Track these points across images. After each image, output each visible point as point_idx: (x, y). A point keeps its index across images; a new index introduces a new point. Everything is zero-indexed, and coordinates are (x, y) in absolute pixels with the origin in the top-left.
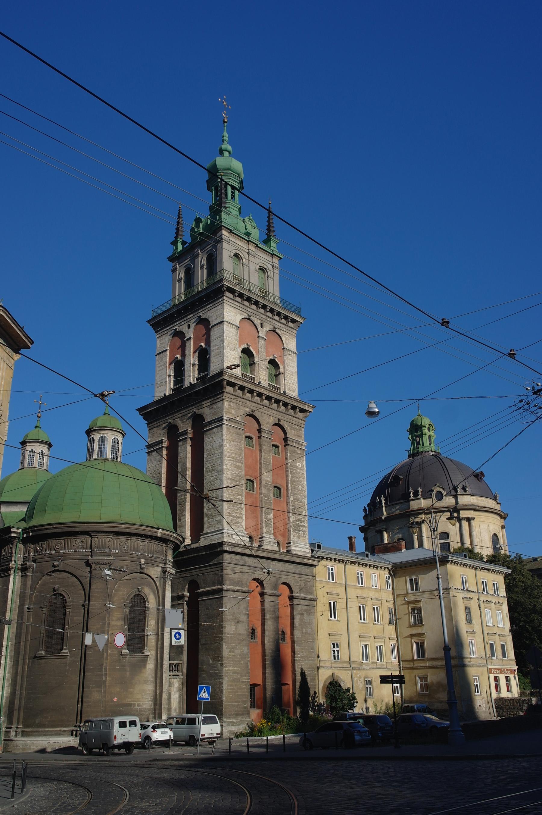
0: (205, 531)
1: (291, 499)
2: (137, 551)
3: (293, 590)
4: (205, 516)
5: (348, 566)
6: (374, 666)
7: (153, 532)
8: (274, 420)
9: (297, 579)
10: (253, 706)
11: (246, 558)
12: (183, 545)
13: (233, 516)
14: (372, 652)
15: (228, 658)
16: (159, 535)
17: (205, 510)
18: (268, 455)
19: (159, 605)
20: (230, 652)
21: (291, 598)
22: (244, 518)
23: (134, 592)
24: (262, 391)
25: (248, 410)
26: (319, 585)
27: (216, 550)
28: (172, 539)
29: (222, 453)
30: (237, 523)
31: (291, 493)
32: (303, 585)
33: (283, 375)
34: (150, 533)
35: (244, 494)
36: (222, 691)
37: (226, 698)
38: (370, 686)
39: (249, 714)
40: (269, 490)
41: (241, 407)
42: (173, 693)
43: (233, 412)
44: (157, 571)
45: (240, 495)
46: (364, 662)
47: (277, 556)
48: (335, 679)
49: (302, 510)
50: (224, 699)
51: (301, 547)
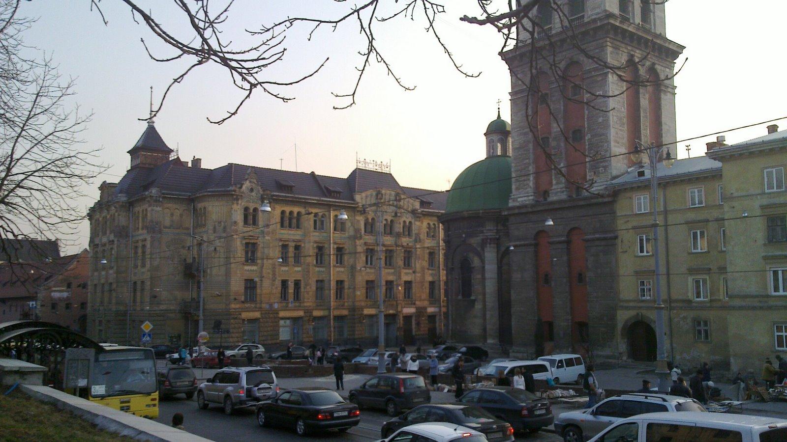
13: (521, 181)
35: (532, 156)
45: (527, 159)
50: (513, 331)
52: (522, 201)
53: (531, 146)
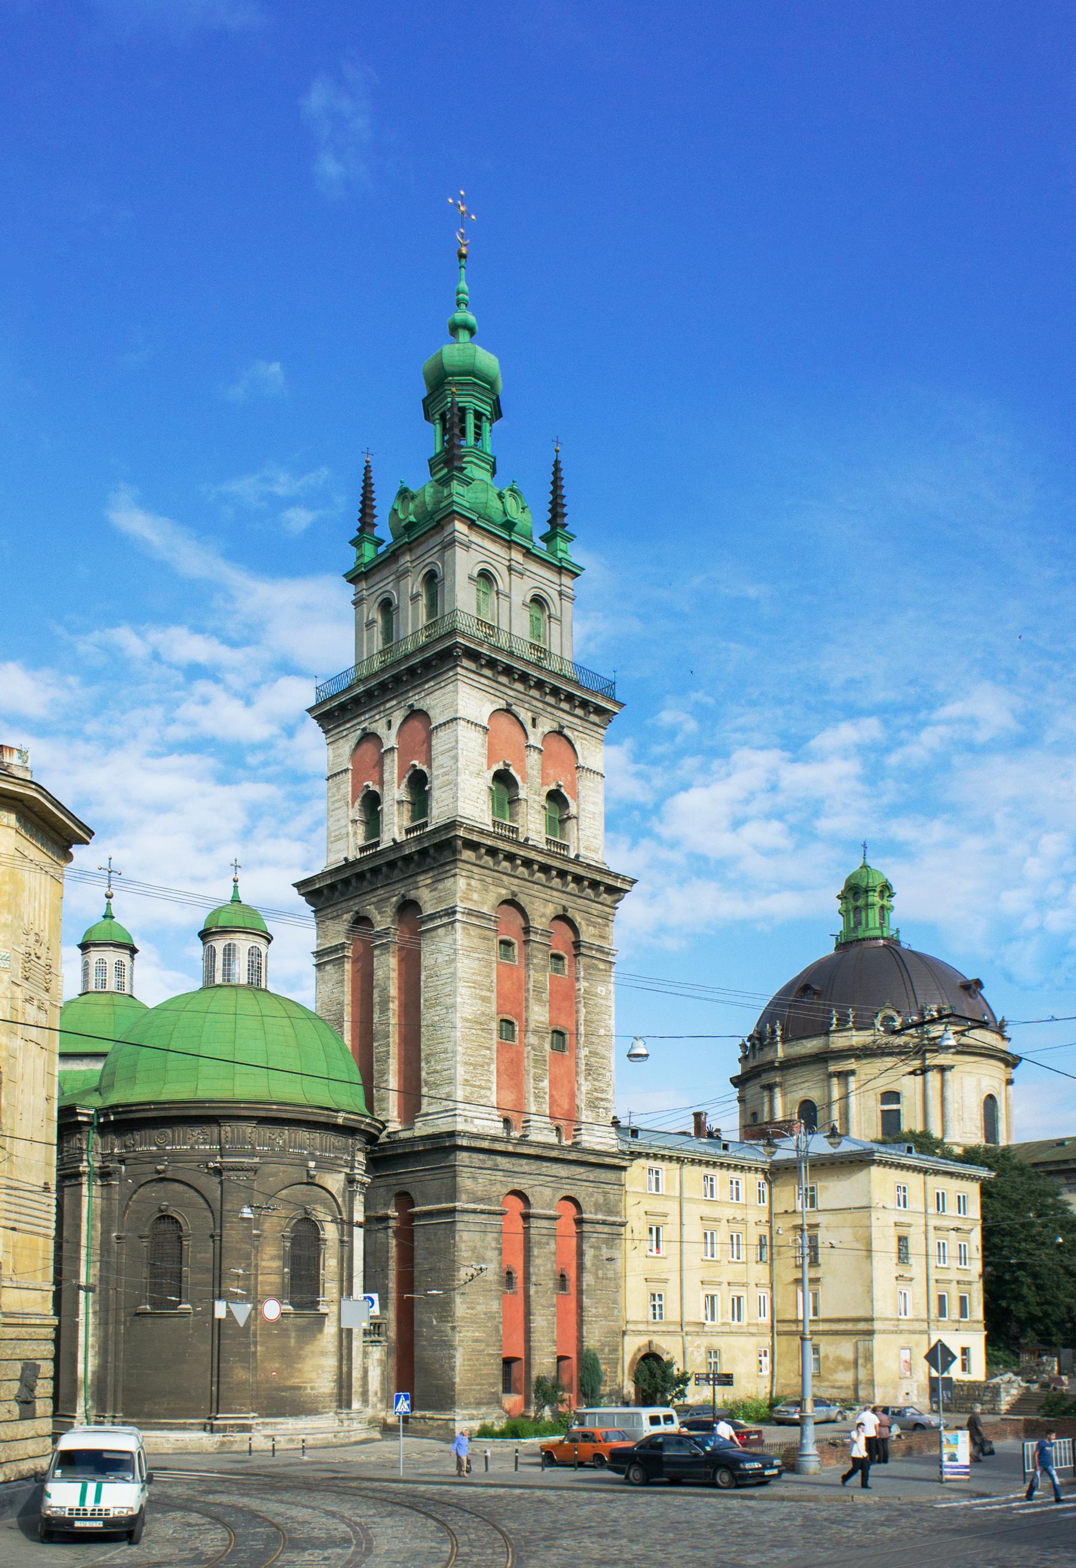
0: (423, 1111)
1: (584, 1052)
2: (301, 1148)
3: (584, 1208)
4: (423, 1084)
5: (688, 1169)
6: (726, 1329)
7: (328, 1116)
8: (555, 908)
9: (590, 1189)
10: (507, 1389)
11: (499, 1159)
12: (385, 1133)
13: (475, 1086)
14: (724, 1306)
15: (464, 1318)
16: (340, 1121)
17: (423, 1074)
18: (540, 976)
19: (342, 1235)
20: (468, 1308)
21: (580, 1222)
22: (494, 1088)
23: (299, 1214)
24: (533, 855)
25: (504, 891)
26: (630, 1200)
27: (443, 1147)
28: (363, 1127)
29: (454, 974)
30: (481, 1097)
31: (585, 1041)
32: (601, 1200)
33: (574, 821)
34: (322, 1119)
35: (495, 1047)
36: (453, 1368)
37: (461, 1379)
38: (716, 1360)
39: (499, 1402)
40: (543, 1038)
41: (491, 887)
42: (371, 1368)
43: (475, 896)
44: (338, 1181)
45: (488, 1049)
46: (709, 1322)
47: (554, 1154)
48: (654, 1349)
49: (603, 1071)
50: (457, 1380)
51: (599, 1138)
52: (483, 1127)
53: (494, 1025)
